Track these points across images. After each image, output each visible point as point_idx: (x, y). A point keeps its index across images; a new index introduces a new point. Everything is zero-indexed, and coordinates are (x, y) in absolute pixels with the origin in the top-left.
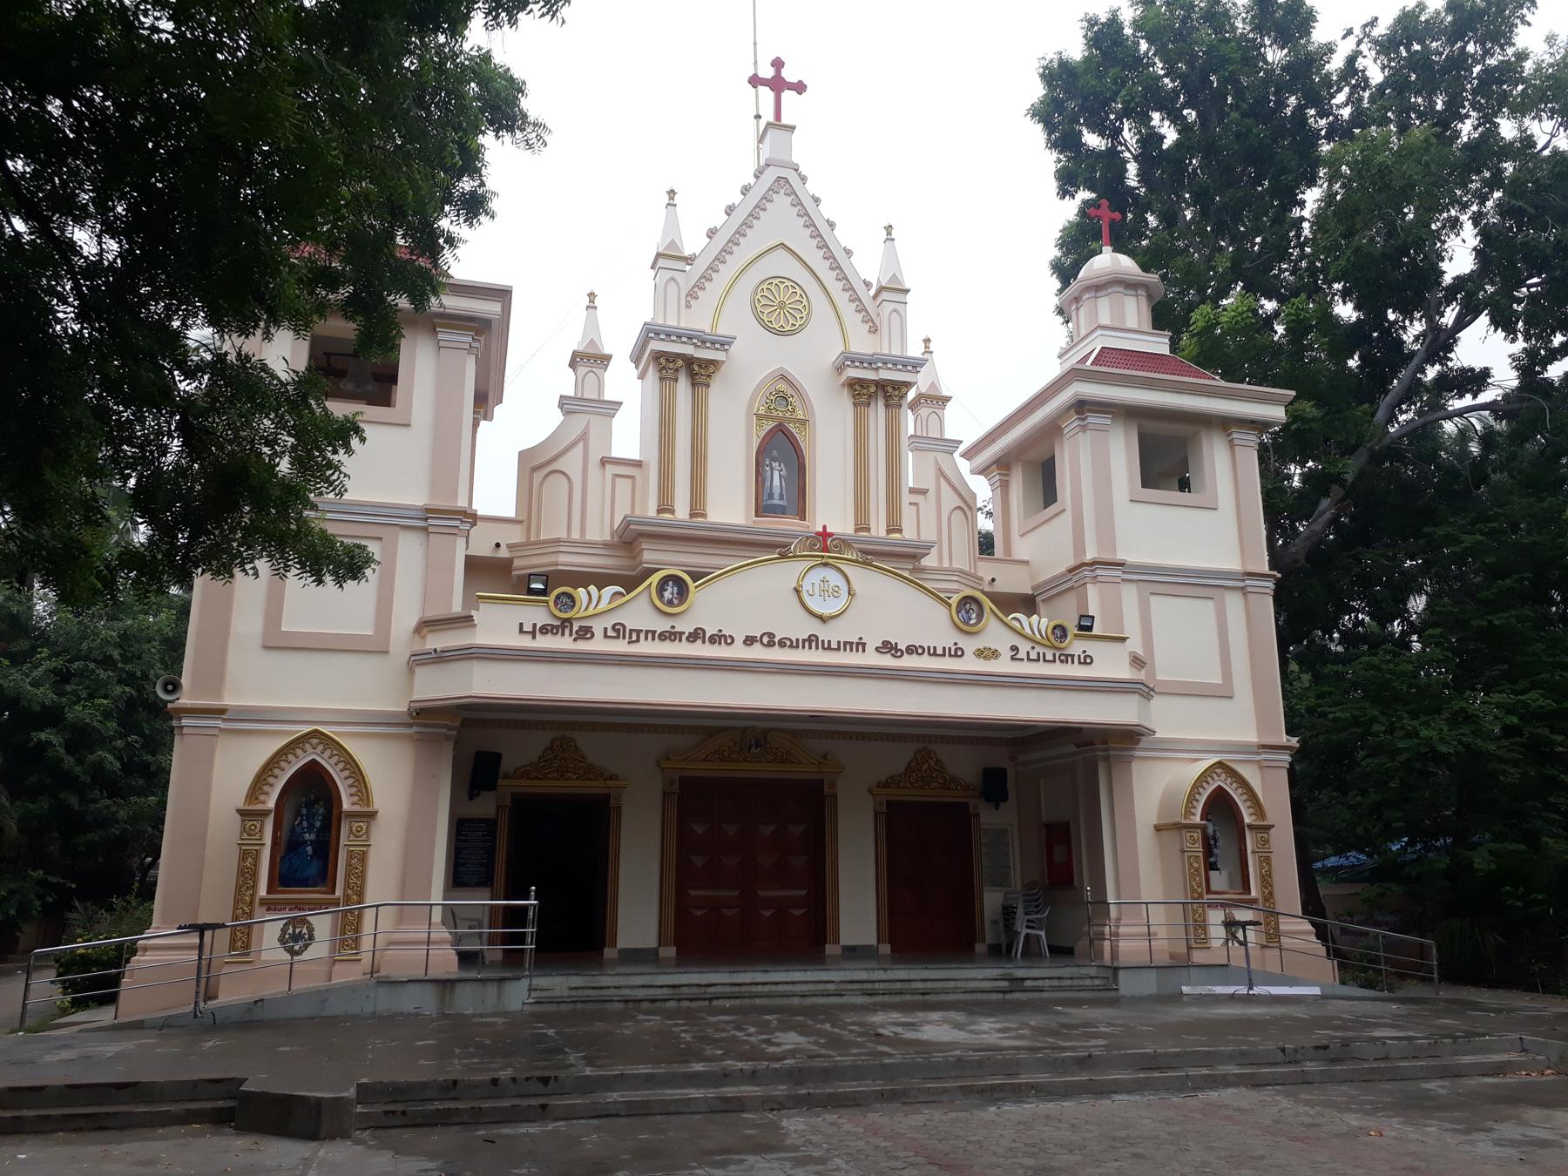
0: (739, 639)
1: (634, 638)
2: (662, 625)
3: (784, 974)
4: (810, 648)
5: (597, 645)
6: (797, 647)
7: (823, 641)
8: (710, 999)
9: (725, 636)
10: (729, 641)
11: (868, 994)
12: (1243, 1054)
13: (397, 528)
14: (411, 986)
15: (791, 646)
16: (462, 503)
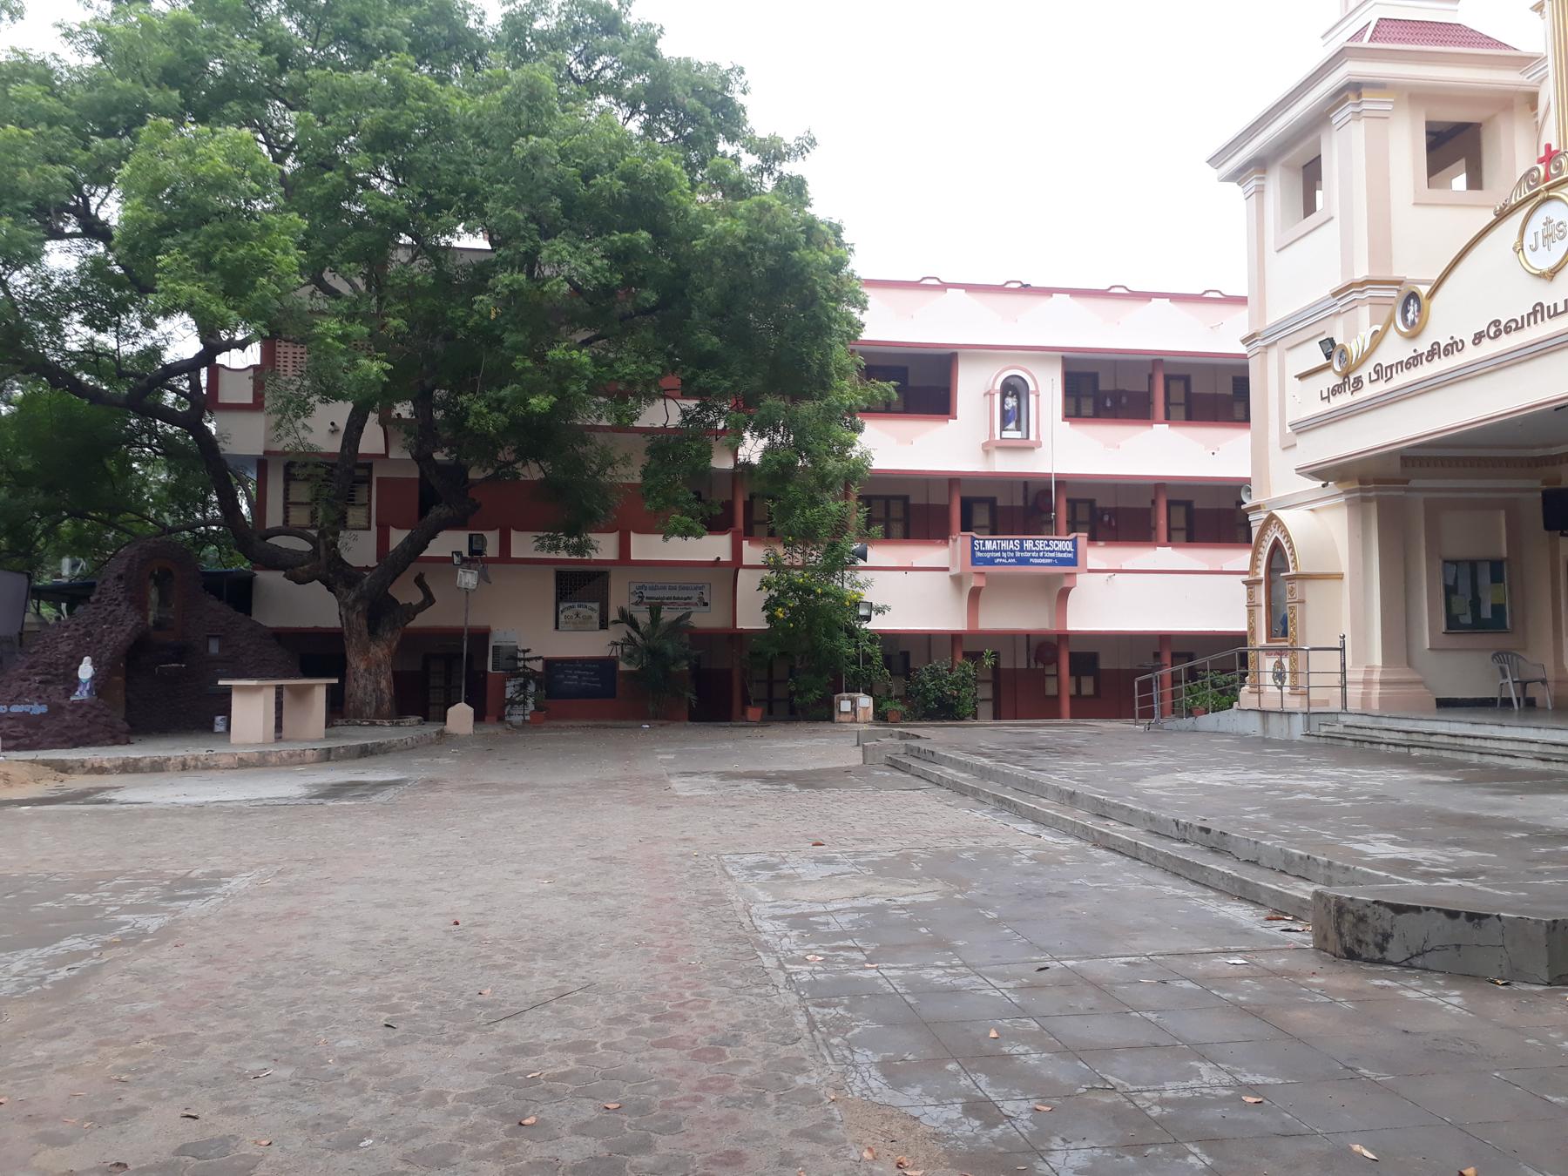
0: (1468, 342)
1: (1389, 376)
2: (1406, 353)
3: (1520, 729)
4: (1536, 322)
5: (1369, 391)
6: (1523, 326)
7: (1549, 307)
8: (1408, 746)
9: (1456, 343)
10: (1460, 346)
11: (1543, 760)
12: (1152, 819)
13: (1329, 319)
14: (1250, 713)
15: (1517, 329)
16: (1361, 273)
